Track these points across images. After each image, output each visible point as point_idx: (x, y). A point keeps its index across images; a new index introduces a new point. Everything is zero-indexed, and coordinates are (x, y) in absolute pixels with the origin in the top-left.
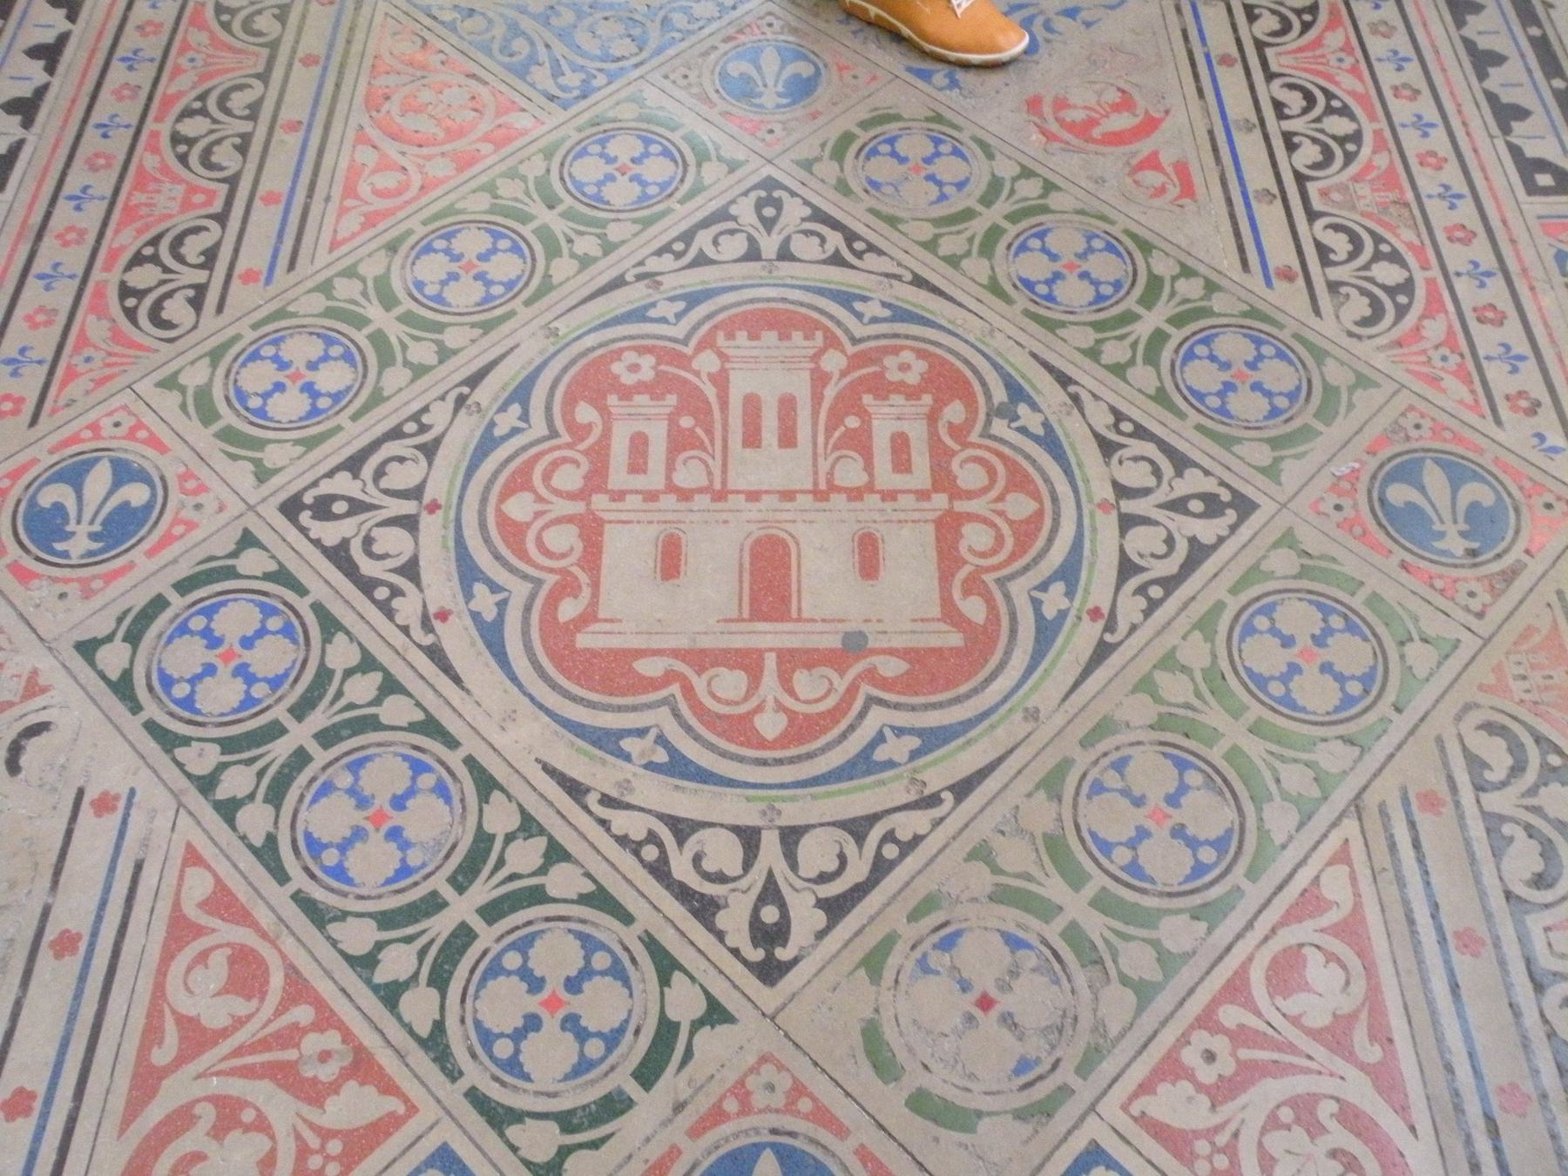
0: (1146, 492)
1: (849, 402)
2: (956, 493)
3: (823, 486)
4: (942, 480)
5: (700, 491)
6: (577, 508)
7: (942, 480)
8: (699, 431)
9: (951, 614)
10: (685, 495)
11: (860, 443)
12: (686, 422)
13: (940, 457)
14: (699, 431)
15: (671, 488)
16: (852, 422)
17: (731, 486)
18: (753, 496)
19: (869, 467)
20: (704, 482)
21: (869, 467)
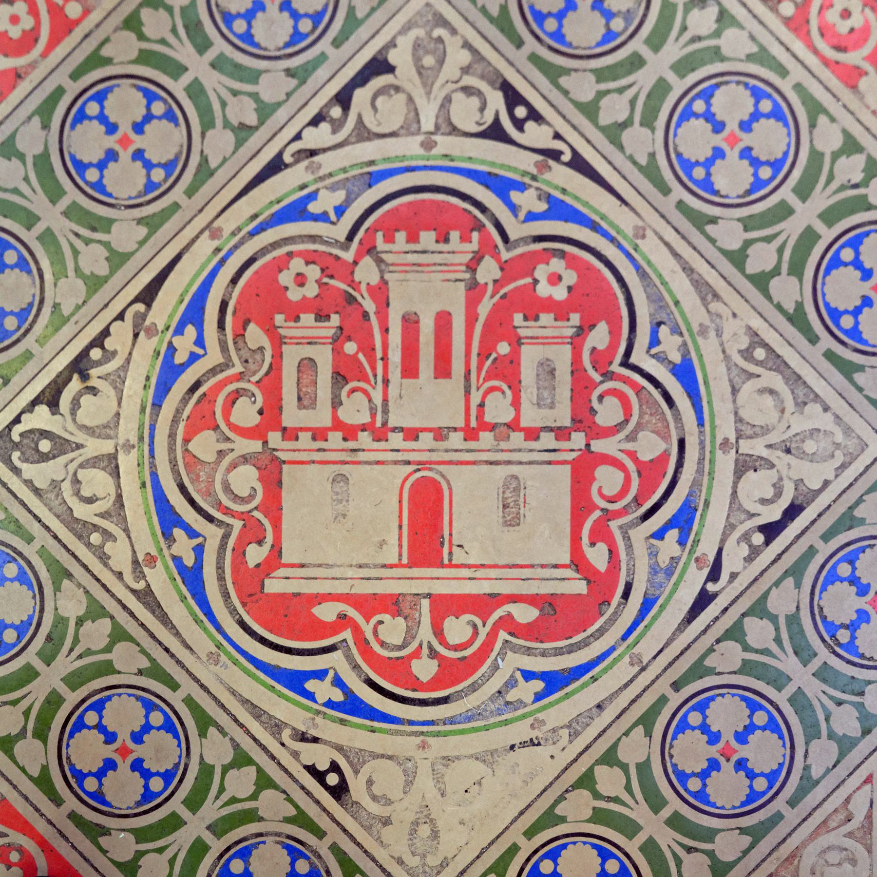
0: (766, 430)
1: (498, 327)
2: (596, 432)
3: (473, 423)
4: (583, 419)
5: (364, 428)
6: (255, 446)
7: (583, 419)
8: (361, 356)
9: (578, 562)
10: (350, 432)
11: (507, 372)
12: (350, 348)
13: (581, 387)
14: (361, 356)
15: (338, 424)
16: (504, 348)
17: (391, 424)
18: (412, 434)
19: (516, 403)
20: (367, 419)
21: (516, 403)
